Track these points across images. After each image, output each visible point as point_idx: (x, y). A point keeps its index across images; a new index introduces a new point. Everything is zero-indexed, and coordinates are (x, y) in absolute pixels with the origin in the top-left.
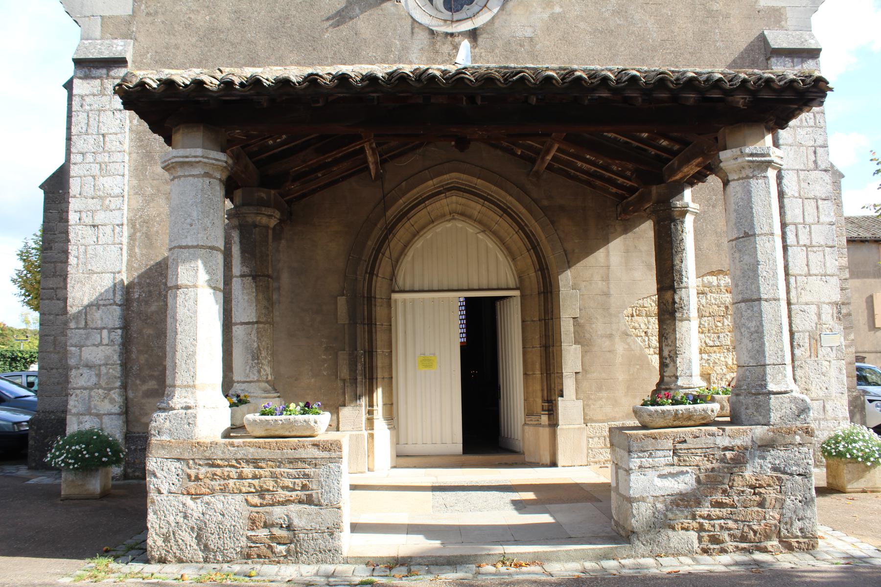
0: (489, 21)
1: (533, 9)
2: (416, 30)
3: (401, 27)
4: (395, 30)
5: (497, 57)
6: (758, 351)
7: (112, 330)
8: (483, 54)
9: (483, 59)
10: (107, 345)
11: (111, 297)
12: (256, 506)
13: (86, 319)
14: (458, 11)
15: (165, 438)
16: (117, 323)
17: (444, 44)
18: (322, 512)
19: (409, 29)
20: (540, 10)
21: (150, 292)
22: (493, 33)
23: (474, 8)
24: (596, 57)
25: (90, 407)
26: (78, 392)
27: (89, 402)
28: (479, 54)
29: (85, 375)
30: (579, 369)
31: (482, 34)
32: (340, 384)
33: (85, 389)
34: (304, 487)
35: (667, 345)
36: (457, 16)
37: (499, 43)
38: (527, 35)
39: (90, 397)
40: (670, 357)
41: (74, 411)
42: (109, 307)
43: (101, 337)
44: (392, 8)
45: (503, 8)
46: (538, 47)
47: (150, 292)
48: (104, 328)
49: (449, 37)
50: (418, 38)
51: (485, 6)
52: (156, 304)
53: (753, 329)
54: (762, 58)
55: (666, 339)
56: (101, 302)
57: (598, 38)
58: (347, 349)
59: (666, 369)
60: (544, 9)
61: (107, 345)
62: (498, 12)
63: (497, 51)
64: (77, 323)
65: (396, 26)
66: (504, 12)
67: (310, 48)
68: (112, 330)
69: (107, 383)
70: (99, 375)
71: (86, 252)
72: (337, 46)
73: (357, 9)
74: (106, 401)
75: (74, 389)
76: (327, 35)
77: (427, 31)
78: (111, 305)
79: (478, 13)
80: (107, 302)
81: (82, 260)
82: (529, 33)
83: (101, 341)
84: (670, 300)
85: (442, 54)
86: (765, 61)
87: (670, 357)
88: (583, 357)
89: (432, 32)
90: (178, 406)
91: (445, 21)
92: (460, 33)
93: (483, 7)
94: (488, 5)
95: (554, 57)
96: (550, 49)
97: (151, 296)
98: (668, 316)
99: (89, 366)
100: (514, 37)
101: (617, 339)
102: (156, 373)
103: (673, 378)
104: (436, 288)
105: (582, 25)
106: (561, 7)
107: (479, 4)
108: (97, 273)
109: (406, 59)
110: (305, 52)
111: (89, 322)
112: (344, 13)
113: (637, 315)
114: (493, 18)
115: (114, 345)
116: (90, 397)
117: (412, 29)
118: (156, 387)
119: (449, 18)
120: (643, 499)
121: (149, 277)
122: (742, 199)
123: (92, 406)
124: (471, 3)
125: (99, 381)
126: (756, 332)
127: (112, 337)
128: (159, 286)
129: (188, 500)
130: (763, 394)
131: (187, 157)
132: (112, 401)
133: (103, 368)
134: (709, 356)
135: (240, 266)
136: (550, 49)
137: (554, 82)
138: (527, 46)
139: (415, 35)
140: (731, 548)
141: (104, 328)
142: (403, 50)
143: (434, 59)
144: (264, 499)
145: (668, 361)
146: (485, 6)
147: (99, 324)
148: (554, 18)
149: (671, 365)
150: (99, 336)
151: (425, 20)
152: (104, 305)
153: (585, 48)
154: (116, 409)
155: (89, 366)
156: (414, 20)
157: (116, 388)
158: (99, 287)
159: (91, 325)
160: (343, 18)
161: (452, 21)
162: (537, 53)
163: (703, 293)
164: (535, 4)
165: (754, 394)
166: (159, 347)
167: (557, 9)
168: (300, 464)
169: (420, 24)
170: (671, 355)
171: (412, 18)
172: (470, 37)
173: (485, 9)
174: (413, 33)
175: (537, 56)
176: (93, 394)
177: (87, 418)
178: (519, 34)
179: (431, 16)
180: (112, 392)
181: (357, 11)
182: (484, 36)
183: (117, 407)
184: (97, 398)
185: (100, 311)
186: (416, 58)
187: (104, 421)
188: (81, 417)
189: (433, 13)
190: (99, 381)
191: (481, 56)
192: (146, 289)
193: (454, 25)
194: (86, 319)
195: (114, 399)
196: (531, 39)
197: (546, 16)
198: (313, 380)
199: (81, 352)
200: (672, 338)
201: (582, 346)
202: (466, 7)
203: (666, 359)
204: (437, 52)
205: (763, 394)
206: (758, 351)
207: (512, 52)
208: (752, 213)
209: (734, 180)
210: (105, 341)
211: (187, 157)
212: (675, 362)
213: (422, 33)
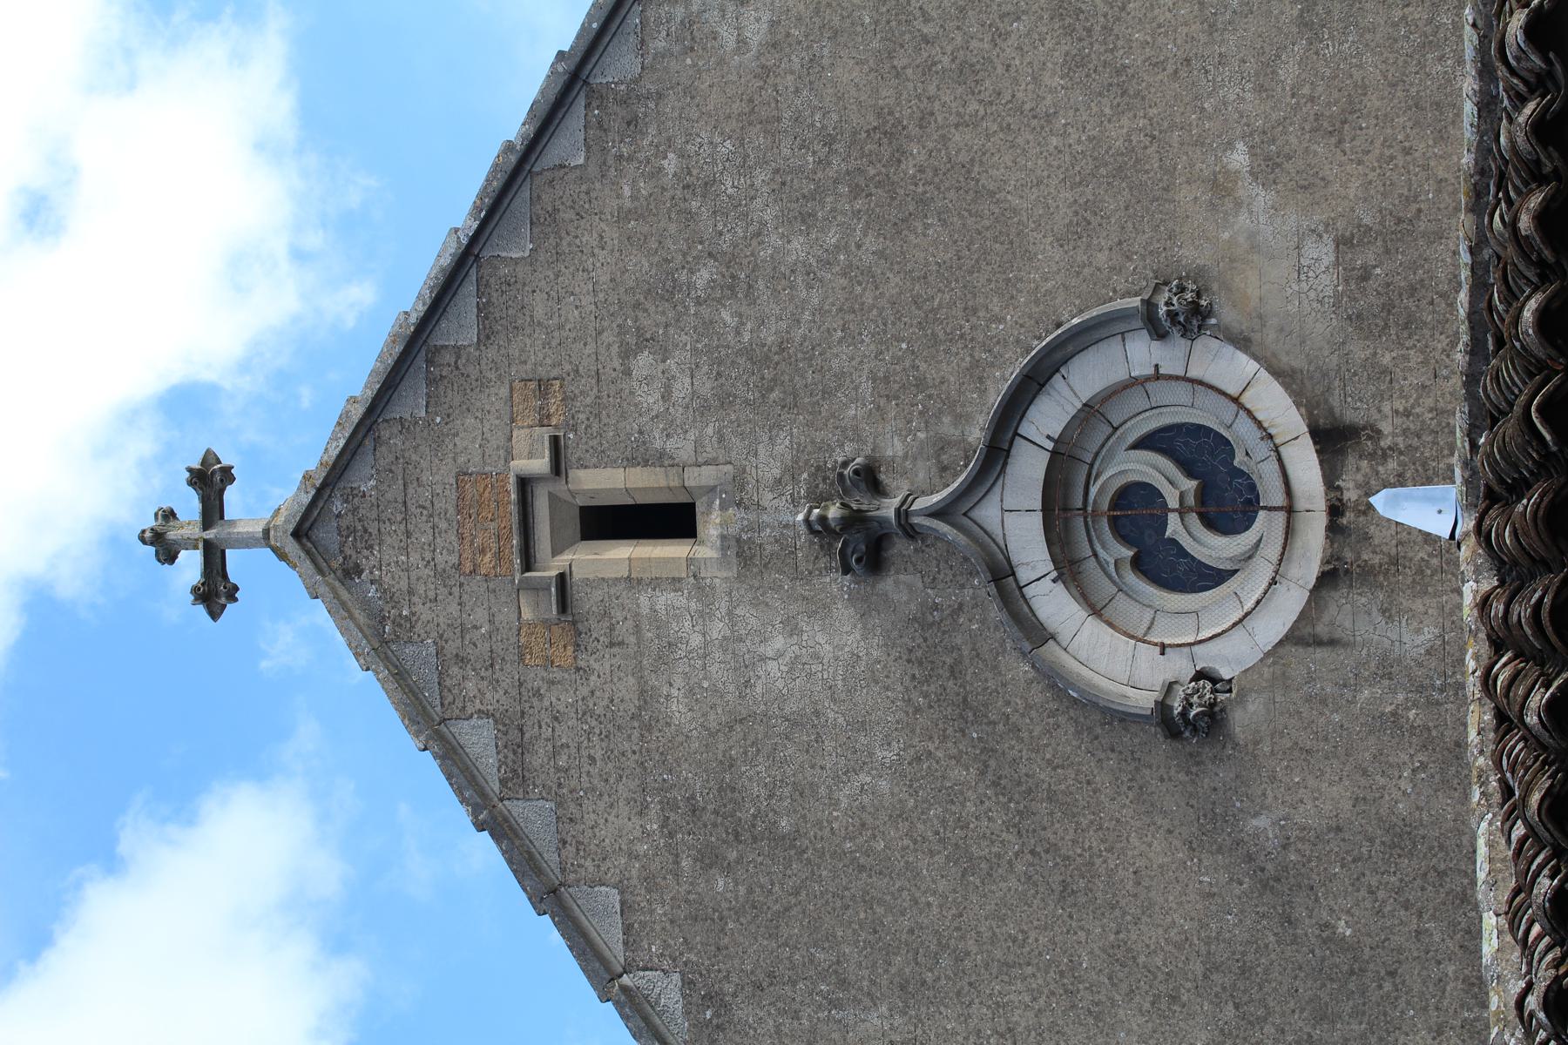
0: (1286, 387)
1: (1241, 239)
2: (1322, 629)
3: (1311, 679)
4: (1324, 702)
5: (1406, 358)
8: (1400, 405)
9: (1417, 403)
14: (1252, 487)
17: (1367, 538)
19: (1320, 653)
20: (1243, 219)
22: (1325, 375)
23: (1242, 433)
28: (1398, 421)
31: (1331, 410)
36: (1272, 494)
37: (1359, 351)
38: (1328, 259)
44: (1251, 708)
45: (1242, 342)
46: (1367, 220)
49: (1344, 520)
50: (1348, 624)
51: (1235, 400)
57: (1329, 12)
60: (1238, 204)
62: (1256, 358)
63: (1387, 359)
65: (1308, 699)
66: (1256, 337)
67: (1388, 986)
72: (1381, 894)
73: (1255, 822)
76: (1343, 929)
77: (1324, 593)
79: (1259, 424)
82: (1321, 253)
85: (1400, 543)
89: (1329, 578)
91: (1289, 532)
92: (1330, 482)
93: (1241, 406)
94: (1233, 390)
95: (1400, 161)
96: (1372, 176)
100: (1337, 305)
105: (1288, 72)
106: (1230, 145)
107: (1228, 419)
109: (1420, 665)
110: (1402, 1004)
112: (1269, 866)
114: (1277, 373)
117: (1319, 643)
119: (1280, 517)
124: (1228, 442)
136: (1372, 176)
137: (1556, 304)
138: (1367, 256)
139: (1338, 634)
142: (1390, 677)
143: (1421, 572)
146: (1235, 400)
148: (1268, 167)
151: (1290, 603)
153: (1368, 58)
156: (1294, 638)
160: (1285, 869)
161: (1290, 510)
162: (1389, 222)
164: (1226, 235)
167: (1239, 158)
169: (1303, 616)
171: (1281, 643)
172: (1342, 452)
173: (1244, 400)
174: (1332, 643)
175: (1399, 221)
178: (1327, 283)
179: (1273, 582)
181: (1262, 822)
182: (1335, 401)
186: (1418, 631)
189: (1261, 572)
191: (1407, 413)
193: (1301, 504)
196: (1343, 243)
197: (1262, 198)
202: (1239, 460)
204: (1395, 561)
207: (1388, 308)
213: (1332, 609)
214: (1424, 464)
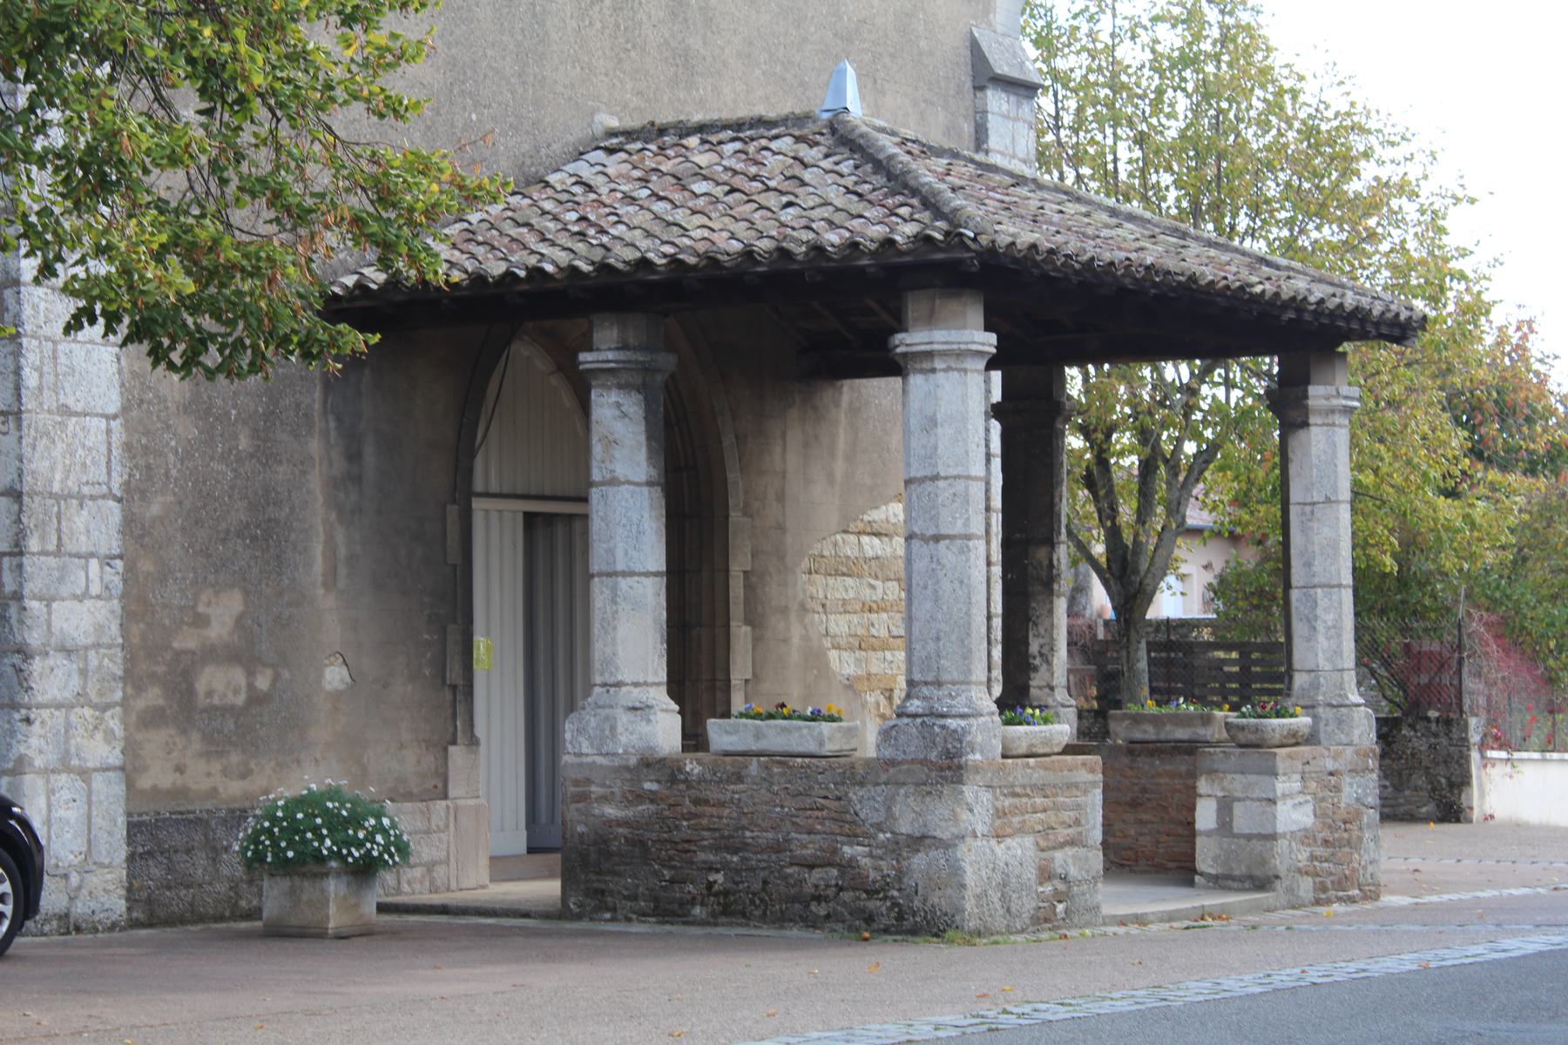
6: (1335, 652)
7: (107, 560)
10: (98, 597)
11: (104, 478)
12: (1043, 850)
13: (59, 530)
15: (978, 756)
16: (115, 544)
18: (1090, 855)
21: (149, 467)
24: (782, 39)
25: (67, 752)
26: (45, 713)
27: (67, 741)
29: (59, 672)
30: (749, 676)
32: (448, 695)
33: (59, 706)
34: (1077, 822)
35: (1037, 636)
39: (68, 726)
40: (1041, 654)
41: (39, 762)
42: (100, 502)
43: (87, 578)
47: (149, 467)
48: (92, 555)
52: (160, 499)
53: (1330, 623)
54: (969, 85)
55: (1036, 625)
56: (86, 490)
58: (460, 621)
59: (1032, 675)
61: (98, 597)
64: (43, 539)
68: (107, 560)
69: (101, 694)
70: (83, 673)
71: (55, 357)
74: (99, 736)
75: (40, 706)
78: (104, 497)
80: (96, 490)
81: (49, 379)
83: (87, 587)
84: (1046, 562)
86: (972, 90)
87: (1041, 654)
88: (754, 648)
90: (985, 711)
97: (150, 478)
98: (1040, 588)
99: (67, 651)
101: (793, 617)
102: (161, 669)
103: (1047, 690)
104: (547, 492)
108: (76, 414)
111: (65, 539)
113: (816, 572)
115: (109, 598)
116: (68, 726)
118: (161, 702)
120: (1284, 835)
121: (147, 433)
122: (1325, 452)
123: (73, 750)
125: (84, 688)
126: (1334, 627)
127: (107, 578)
128: (166, 457)
129: (993, 842)
130: (1346, 706)
131: (983, 344)
132: (109, 736)
133: (92, 654)
134: (893, 655)
135: (644, 464)
140: (1334, 899)
141: (92, 555)
144: (1048, 839)
145: (1037, 662)
147: (84, 545)
149: (1044, 668)
150: (83, 574)
152: (92, 498)
154: (115, 758)
155: (67, 651)
157: (115, 704)
158: (80, 451)
159: (70, 547)
163: (886, 535)
165: (1334, 706)
166: (165, 606)
168: (1075, 792)
170: (1044, 651)
176: (73, 718)
177: (64, 777)
180: (108, 714)
183: (118, 751)
184: (81, 731)
185: (85, 513)
187: (94, 785)
188: (53, 777)
190: (84, 688)
192: (142, 462)
194: (59, 530)
195: (112, 731)
198: (410, 687)
199: (49, 613)
200: (1047, 623)
201: (754, 627)
203: (1034, 658)
205: (1346, 706)
206: (1335, 652)
208: (1335, 472)
209: (1316, 425)
210: (95, 589)
211: (983, 344)
212: (1049, 663)
214: (621, 9)
